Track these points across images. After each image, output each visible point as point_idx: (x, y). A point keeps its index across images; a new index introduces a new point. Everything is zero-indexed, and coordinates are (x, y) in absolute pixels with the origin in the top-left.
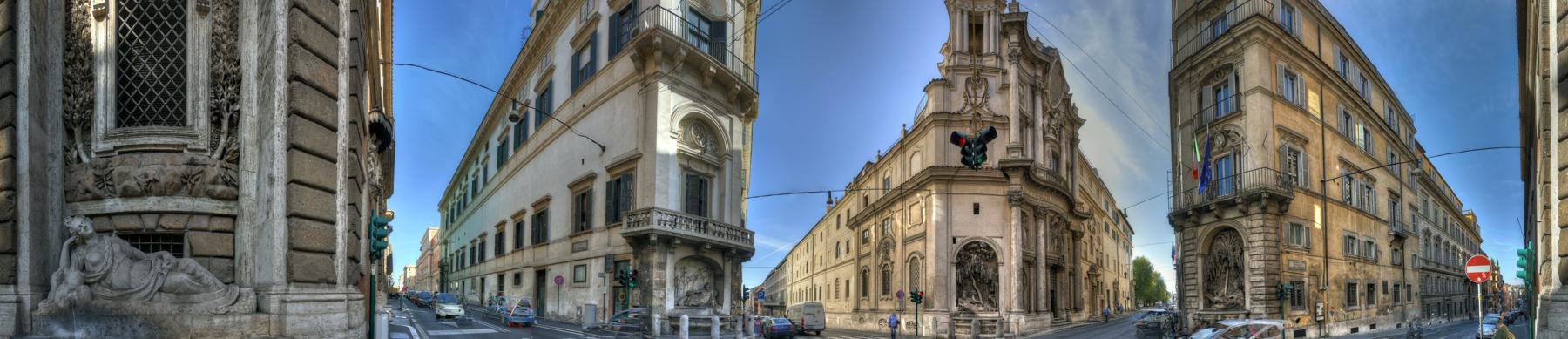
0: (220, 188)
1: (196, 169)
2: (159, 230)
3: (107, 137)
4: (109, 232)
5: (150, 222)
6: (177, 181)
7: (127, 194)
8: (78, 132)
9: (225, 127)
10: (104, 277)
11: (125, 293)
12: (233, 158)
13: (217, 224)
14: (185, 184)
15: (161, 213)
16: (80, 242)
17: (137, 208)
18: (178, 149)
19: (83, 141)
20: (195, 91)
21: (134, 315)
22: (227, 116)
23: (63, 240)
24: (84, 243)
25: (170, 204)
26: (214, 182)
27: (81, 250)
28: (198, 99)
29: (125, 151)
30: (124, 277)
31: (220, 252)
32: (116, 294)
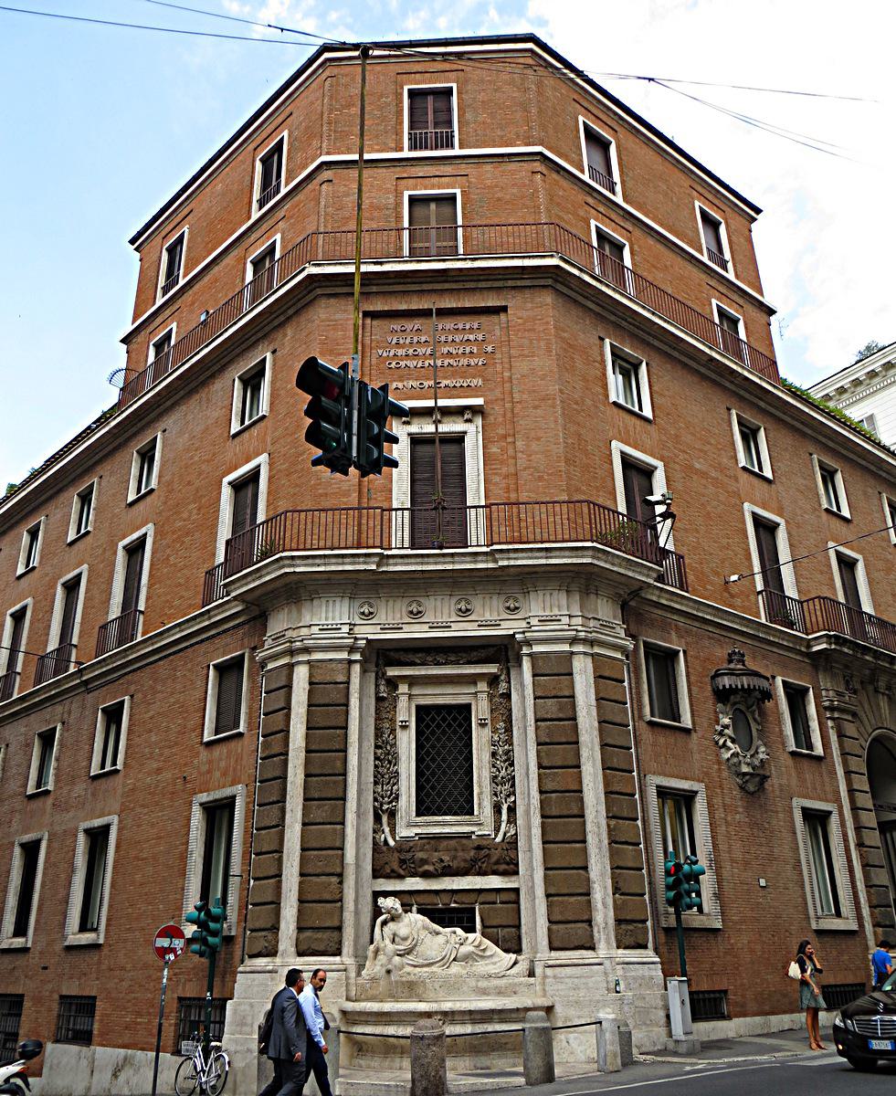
0: (503, 867)
1: (483, 852)
3: (409, 825)
7: (426, 875)
13: (505, 897)
22: (505, 807)
27: (391, 925)
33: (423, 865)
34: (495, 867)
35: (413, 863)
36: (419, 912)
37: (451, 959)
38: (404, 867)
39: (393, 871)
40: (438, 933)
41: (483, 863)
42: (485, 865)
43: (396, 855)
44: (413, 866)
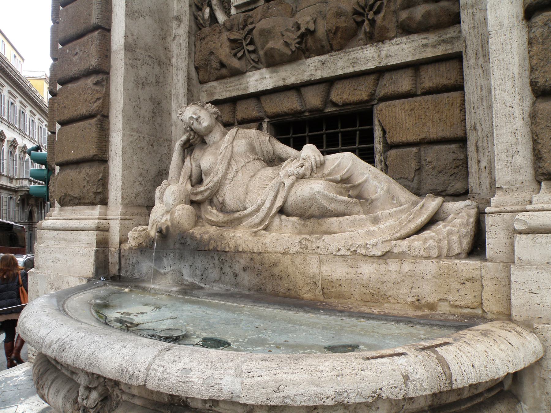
2: (330, 110)
5: (313, 99)
6: (343, 23)
7: (273, 62)
10: (216, 191)
16: (195, 142)
17: (292, 80)
24: (204, 142)
25: (339, 64)
27: (197, 153)
30: (240, 192)
33: (267, 42)
34: (404, 15)
35: (252, 43)
37: (275, 210)
39: (222, 65)
41: (377, 12)
43: (225, 35)
44: (251, 48)
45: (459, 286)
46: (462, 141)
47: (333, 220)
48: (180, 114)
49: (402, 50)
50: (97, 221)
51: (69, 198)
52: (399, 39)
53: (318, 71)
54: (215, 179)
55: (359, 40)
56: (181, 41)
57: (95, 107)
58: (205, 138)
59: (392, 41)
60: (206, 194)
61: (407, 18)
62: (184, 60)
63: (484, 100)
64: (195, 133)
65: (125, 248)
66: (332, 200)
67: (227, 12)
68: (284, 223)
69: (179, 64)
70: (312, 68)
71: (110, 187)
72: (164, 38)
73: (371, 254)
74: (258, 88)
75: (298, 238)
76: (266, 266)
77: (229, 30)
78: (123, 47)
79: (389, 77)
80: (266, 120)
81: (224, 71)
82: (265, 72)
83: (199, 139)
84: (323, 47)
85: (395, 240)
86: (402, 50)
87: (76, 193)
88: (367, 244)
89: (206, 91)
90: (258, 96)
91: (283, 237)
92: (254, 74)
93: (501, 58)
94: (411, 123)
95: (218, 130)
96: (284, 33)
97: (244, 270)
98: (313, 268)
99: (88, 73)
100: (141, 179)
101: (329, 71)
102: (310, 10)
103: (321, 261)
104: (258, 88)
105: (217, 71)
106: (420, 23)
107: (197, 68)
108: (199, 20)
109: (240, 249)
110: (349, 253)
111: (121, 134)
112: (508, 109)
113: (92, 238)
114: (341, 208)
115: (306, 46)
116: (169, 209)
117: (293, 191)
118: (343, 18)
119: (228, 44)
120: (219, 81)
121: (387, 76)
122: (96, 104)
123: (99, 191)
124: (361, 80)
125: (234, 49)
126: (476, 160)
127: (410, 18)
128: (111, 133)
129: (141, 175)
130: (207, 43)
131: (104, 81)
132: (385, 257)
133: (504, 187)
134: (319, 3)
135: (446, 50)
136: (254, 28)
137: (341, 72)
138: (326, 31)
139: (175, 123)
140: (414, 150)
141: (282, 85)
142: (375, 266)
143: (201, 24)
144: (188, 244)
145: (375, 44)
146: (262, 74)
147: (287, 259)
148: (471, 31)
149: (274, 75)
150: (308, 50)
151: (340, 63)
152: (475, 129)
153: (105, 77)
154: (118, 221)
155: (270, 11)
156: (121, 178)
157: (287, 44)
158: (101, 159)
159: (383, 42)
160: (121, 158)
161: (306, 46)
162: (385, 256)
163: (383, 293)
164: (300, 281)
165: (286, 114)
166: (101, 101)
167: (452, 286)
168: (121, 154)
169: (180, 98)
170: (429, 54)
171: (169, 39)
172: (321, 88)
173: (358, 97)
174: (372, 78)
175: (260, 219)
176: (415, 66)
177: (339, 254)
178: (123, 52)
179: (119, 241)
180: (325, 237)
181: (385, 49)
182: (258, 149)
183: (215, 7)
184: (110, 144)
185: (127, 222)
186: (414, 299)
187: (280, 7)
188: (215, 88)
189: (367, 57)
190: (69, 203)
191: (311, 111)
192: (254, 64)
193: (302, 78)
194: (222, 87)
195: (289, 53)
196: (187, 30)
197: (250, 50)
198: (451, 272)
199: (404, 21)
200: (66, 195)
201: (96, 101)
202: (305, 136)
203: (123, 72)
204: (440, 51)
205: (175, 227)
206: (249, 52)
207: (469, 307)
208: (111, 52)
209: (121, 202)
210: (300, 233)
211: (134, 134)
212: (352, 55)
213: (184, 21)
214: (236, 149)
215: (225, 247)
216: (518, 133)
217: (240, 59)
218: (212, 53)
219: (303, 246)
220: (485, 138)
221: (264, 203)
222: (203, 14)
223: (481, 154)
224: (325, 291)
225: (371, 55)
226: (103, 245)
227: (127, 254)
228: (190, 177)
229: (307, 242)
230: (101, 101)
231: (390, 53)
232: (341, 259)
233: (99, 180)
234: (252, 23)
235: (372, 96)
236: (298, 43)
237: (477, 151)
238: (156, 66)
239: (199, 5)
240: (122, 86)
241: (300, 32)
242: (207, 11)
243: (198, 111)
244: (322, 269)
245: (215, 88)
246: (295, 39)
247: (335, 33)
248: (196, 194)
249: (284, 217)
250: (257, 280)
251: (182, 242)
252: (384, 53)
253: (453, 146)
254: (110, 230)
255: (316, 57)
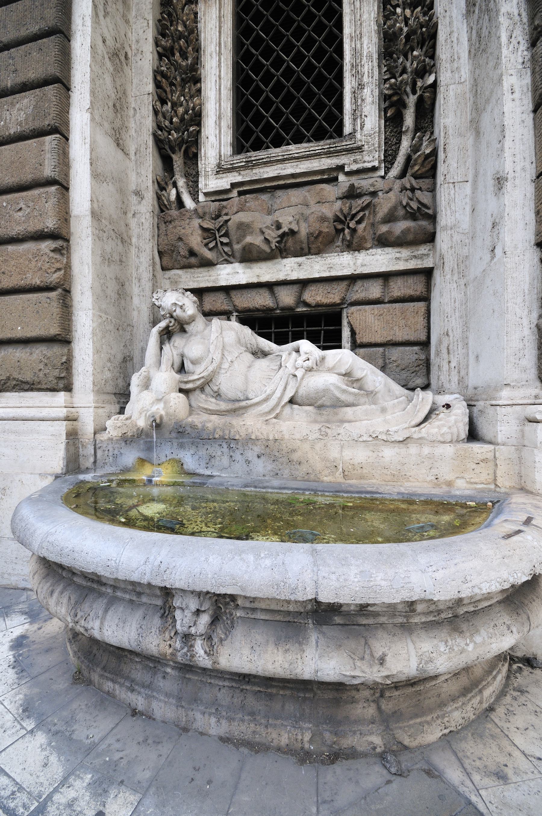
0: (401, 226)
3: (221, 170)
4: (226, 314)
5: (287, 298)
6: (326, 228)
7: (249, 257)
8: (178, 160)
9: (409, 120)
11: (238, 407)
12: (425, 169)
14: (342, 233)
15: (304, 284)
16: (175, 329)
18: (329, 177)
19: (187, 175)
20: (357, 74)
21: (250, 441)
22: (412, 100)
23: (154, 323)
24: (183, 330)
26: (390, 218)
27: (178, 341)
28: (361, 86)
29: (246, 190)
31: (401, 335)
32: (223, 406)
33: (244, 236)
34: (384, 228)
35: (226, 235)
36: (243, 321)
37: (286, 399)
38: (211, 245)
39: (192, 253)
40: (265, 354)
41: (359, 222)
42: (362, 226)
43: (196, 222)
44: (225, 240)
45: (475, 466)
46: (425, 344)
47: (348, 409)
48: (157, 299)
49: (379, 260)
50: (65, 410)
51: (14, 382)
52: (374, 250)
53: (294, 272)
54: (211, 369)
55: (337, 247)
56: (143, 220)
57: (55, 277)
58: (185, 326)
59: (368, 252)
60: (198, 383)
61: (387, 232)
62: (147, 241)
63: (457, 311)
64: (175, 320)
65: (102, 439)
66: (344, 391)
67: (194, 196)
68: (295, 412)
69: (141, 245)
70: (288, 268)
71: (74, 371)
72: (125, 213)
73: (393, 440)
74: (229, 281)
75: (317, 427)
76: (283, 452)
77: (202, 218)
78: (88, 213)
79: (361, 284)
80: (235, 314)
81: (193, 260)
82: (237, 266)
83: (178, 327)
84: (302, 249)
85: (414, 427)
86: (379, 260)
87: (28, 376)
88: (388, 431)
89: (169, 278)
90: (227, 290)
91: (297, 426)
92: (225, 267)
93: (514, 275)
94: (379, 327)
95: (201, 320)
96: (264, 230)
97: (259, 457)
98: (334, 453)
99: (40, 236)
100: (109, 364)
101: (306, 273)
102: (292, 210)
103: (342, 447)
104: (229, 281)
105: (184, 260)
106: (398, 237)
107: (160, 253)
108: (163, 201)
109: (253, 437)
110: (371, 439)
111: (90, 313)
112: (518, 319)
113: (62, 428)
114: (349, 399)
115: (285, 246)
116: (160, 397)
117: (304, 383)
118: (326, 224)
119: (200, 232)
120: (185, 270)
121: (359, 283)
122: (56, 275)
123: (62, 375)
124: (335, 285)
125: (205, 239)
126: (447, 361)
127: (389, 232)
128: (74, 312)
129: (109, 360)
130: (175, 227)
131: (64, 249)
132: (405, 442)
133: (512, 384)
134: (301, 204)
135: (417, 265)
136: (229, 220)
137: (317, 275)
138: (308, 234)
139: (138, 308)
140: (381, 349)
141: (256, 282)
142: (396, 450)
143: (165, 205)
144: (187, 432)
145: (351, 252)
146: (234, 268)
147: (306, 446)
148: (449, 250)
149: (249, 270)
150: (285, 250)
151: (317, 267)
152: (448, 335)
153: (65, 244)
154: (91, 410)
155: (248, 204)
156: (91, 362)
157: (267, 241)
158: (63, 339)
159: (359, 251)
160: (91, 341)
161: (285, 246)
162: (405, 441)
163: (403, 474)
164: (319, 466)
165: (257, 310)
166: (62, 272)
167: (468, 466)
168: (91, 336)
169: (143, 282)
170: (401, 266)
171: (130, 215)
172: (295, 288)
173: (331, 300)
174: (344, 284)
175: (270, 408)
176: (385, 277)
177: (361, 439)
178: (89, 218)
179: (93, 431)
180: (346, 425)
181: (361, 258)
182: (243, 341)
183: (181, 190)
184: (74, 323)
185: (100, 410)
186: (433, 478)
187: (257, 203)
188: (180, 277)
189: (343, 263)
190: (14, 388)
191: (283, 309)
192: (226, 257)
193: (277, 277)
194: (189, 277)
195: (268, 250)
196: (150, 208)
197: (223, 242)
198: (467, 454)
199: (383, 234)
200: (8, 378)
201: (55, 271)
202: (271, 332)
203: (90, 243)
204: (412, 265)
205: (171, 416)
206: (222, 243)
207: (483, 483)
208: (70, 216)
209: (92, 388)
210: (315, 421)
211: (103, 315)
212: (329, 260)
213: (147, 199)
214: (226, 340)
215: (235, 435)
216: (526, 340)
217: (210, 250)
218: (180, 239)
219: (323, 433)
220: (456, 343)
221: (274, 393)
222: (169, 195)
223: (452, 356)
224: (346, 473)
225: (347, 262)
226: (73, 436)
227: (105, 446)
228: (172, 365)
229: (327, 430)
230: (62, 272)
231: (365, 263)
232: (363, 444)
233: (62, 364)
234: (226, 214)
235: (343, 299)
236: (277, 242)
237: (449, 353)
238: (119, 243)
239: (163, 183)
240: (90, 258)
241: (281, 232)
242: (174, 192)
243: (180, 298)
244: (344, 454)
245: (180, 277)
246: (276, 238)
247: (316, 238)
248: (186, 382)
249: (295, 406)
250: (273, 466)
251: (181, 430)
252: (359, 262)
253: (416, 348)
254: (79, 419)
255: (293, 258)
